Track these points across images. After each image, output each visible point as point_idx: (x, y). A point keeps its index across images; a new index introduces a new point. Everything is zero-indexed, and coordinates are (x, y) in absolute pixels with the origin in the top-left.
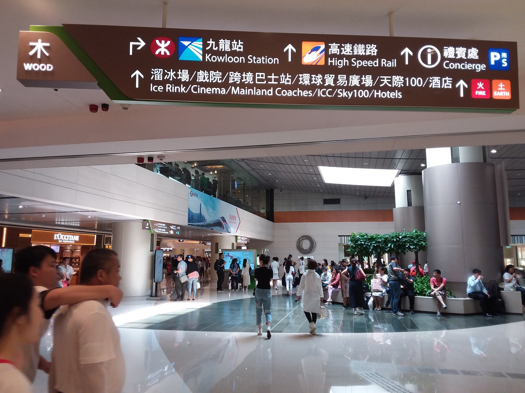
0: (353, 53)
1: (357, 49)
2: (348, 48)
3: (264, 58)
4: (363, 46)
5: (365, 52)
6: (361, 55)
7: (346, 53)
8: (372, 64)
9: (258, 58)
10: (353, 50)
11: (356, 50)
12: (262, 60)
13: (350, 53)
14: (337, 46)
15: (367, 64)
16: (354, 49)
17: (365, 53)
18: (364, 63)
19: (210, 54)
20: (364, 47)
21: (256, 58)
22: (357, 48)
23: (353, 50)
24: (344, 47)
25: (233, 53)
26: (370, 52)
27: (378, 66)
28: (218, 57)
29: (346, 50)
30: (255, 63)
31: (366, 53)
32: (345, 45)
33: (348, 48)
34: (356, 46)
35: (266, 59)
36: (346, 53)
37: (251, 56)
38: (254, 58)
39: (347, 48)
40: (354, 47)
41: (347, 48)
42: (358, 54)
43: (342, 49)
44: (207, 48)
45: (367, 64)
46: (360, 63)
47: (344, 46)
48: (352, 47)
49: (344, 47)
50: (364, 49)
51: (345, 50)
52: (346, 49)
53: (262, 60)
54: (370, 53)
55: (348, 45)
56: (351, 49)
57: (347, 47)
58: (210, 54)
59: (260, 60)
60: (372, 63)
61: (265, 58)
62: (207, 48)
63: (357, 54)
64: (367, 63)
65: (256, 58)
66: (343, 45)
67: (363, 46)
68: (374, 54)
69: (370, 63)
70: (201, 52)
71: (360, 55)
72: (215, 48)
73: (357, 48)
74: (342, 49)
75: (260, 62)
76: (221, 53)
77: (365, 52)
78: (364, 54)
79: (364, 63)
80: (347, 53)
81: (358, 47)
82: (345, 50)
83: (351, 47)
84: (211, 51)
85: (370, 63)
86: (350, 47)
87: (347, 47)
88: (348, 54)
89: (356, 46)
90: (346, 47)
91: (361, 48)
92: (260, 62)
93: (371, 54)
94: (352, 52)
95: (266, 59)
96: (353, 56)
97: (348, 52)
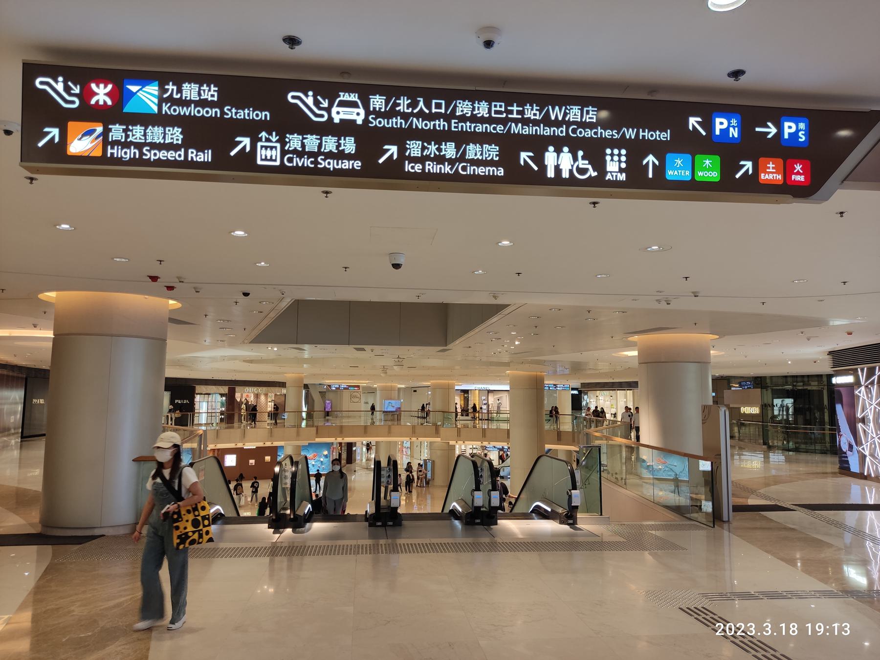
0: (146, 139)
1: (152, 134)
2: (138, 132)
3: (248, 112)
4: (160, 130)
5: (164, 138)
6: (158, 142)
7: (134, 139)
8: (175, 157)
9: (238, 111)
10: (145, 135)
11: (150, 136)
12: (244, 113)
13: (140, 139)
14: (121, 130)
15: (167, 157)
16: (147, 134)
17: (163, 140)
18: (162, 155)
19: (169, 104)
20: (163, 132)
21: (236, 111)
22: (151, 133)
23: (145, 135)
24: (132, 131)
25: (203, 103)
26: (172, 138)
27: (183, 159)
28: (180, 108)
29: (135, 135)
30: (235, 117)
31: (165, 140)
32: (134, 128)
33: (138, 132)
34: (150, 129)
35: (251, 112)
36: (134, 139)
37: (230, 108)
38: (234, 110)
39: (136, 132)
40: (147, 131)
41: (136, 132)
42: (154, 141)
43: (128, 133)
44: (165, 96)
45: (167, 157)
46: (155, 155)
47: (132, 130)
48: (145, 130)
49: (132, 131)
50: (163, 135)
51: (133, 135)
52: (134, 133)
53: (244, 113)
54: (172, 141)
55: (138, 127)
56: (142, 134)
57: (136, 131)
58: (169, 104)
59: (242, 114)
60: (174, 155)
61: (250, 111)
62: (165, 96)
63: (151, 141)
64: (166, 155)
65: (236, 111)
66: (130, 127)
67: (160, 130)
68: (177, 142)
69: (171, 155)
70: (156, 101)
71: (155, 143)
72: (177, 94)
73: (151, 133)
74: (128, 133)
75: (242, 117)
76: (186, 103)
77: (164, 138)
78: (162, 142)
79: (161, 155)
80: (136, 139)
81: (153, 131)
82: (133, 135)
83: (142, 131)
84: (170, 99)
85: (171, 155)
86: (141, 131)
87: (136, 131)
88: (138, 141)
89: (150, 129)
90: (134, 131)
91: (158, 133)
92: (242, 117)
93: (172, 143)
94: (143, 138)
95: (251, 112)
96: (145, 144)
97: (138, 138)
